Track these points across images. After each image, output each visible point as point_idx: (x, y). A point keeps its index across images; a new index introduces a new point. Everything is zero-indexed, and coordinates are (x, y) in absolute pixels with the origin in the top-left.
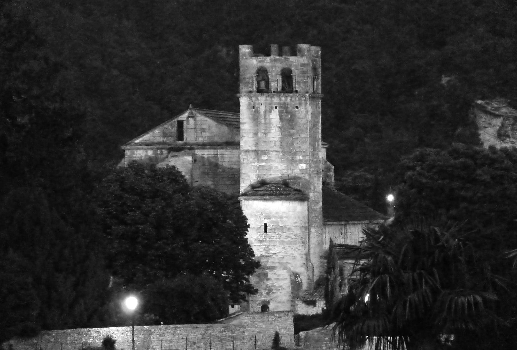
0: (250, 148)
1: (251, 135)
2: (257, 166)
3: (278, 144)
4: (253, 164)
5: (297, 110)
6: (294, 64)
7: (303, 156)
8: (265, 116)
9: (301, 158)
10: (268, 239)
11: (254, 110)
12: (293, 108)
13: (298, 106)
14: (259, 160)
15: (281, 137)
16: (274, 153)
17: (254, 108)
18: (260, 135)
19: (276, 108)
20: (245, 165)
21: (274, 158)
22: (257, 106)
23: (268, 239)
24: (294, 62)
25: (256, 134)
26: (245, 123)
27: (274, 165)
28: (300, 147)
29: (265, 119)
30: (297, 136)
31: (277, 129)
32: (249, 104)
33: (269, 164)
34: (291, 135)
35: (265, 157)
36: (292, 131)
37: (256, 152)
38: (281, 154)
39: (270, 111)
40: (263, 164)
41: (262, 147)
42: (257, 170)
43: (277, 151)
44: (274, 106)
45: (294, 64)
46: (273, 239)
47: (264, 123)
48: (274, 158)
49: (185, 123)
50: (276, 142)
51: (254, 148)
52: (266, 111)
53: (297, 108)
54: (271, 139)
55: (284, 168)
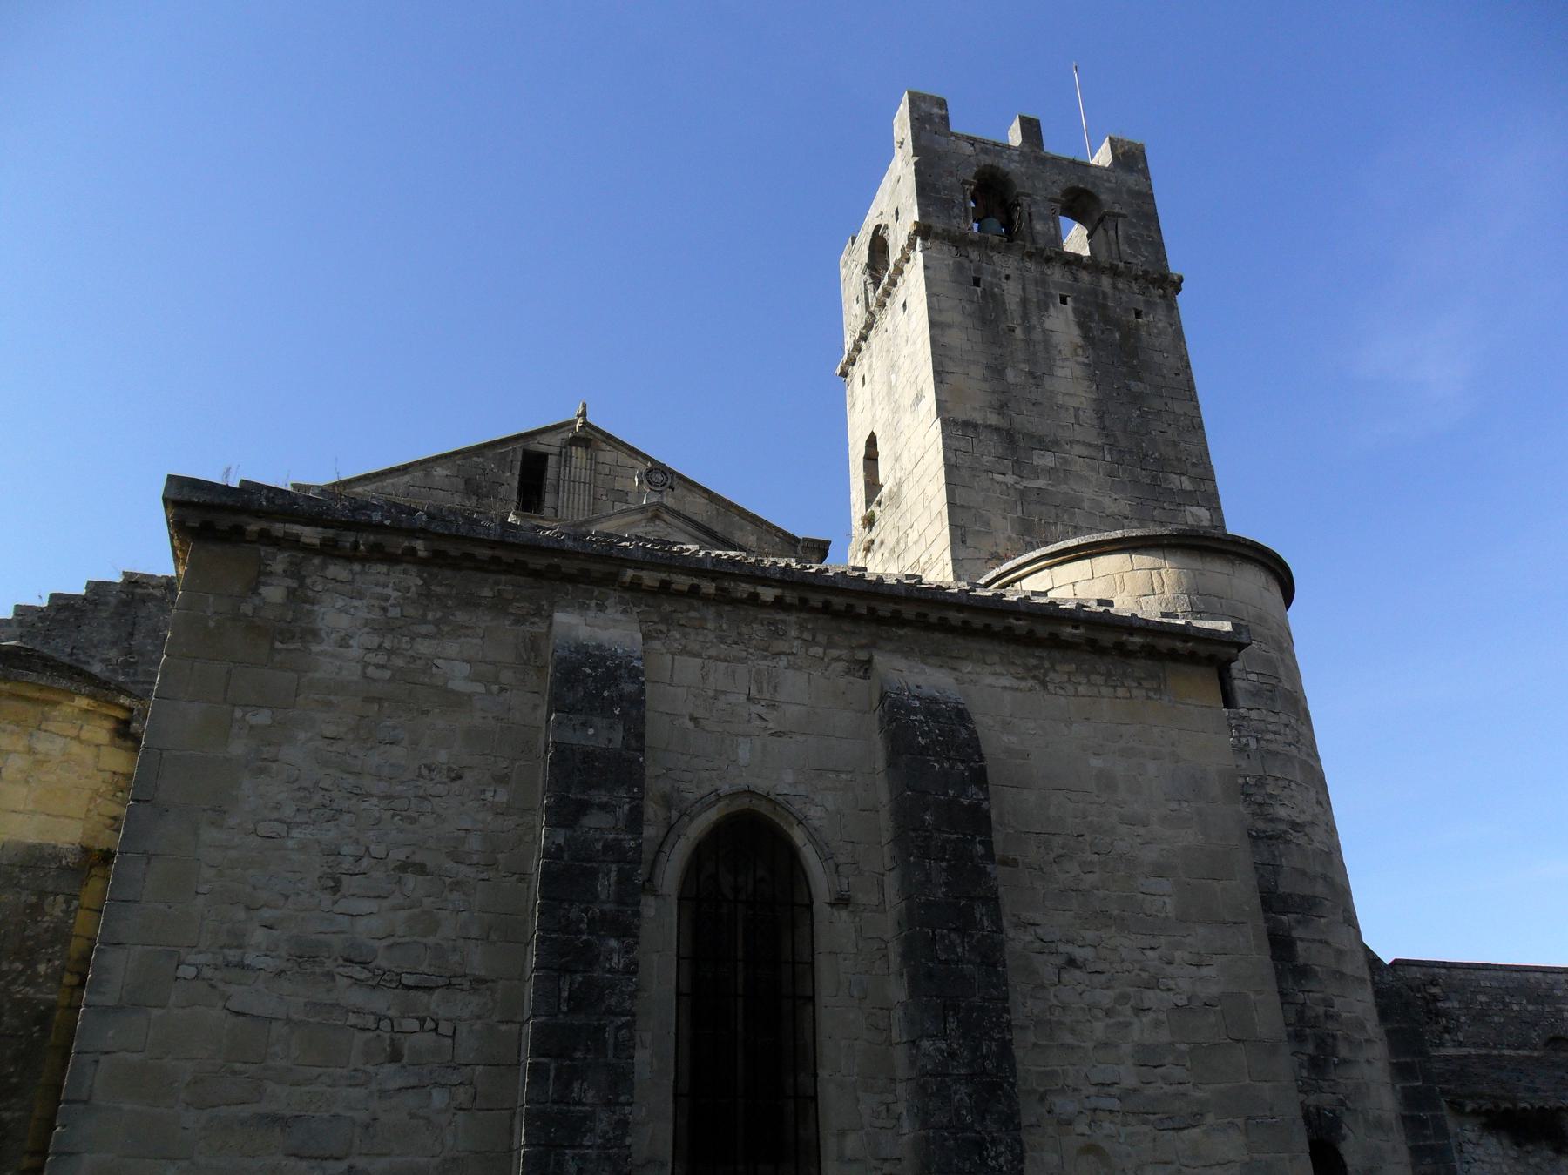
0: (978, 418)
1: (977, 372)
2: (1017, 486)
3: (1088, 416)
4: (997, 477)
5: (1140, 320)
6: (1107, 184)
7: (1192, 479)
8: (1025, 317)
9: (1187, 484)
10: (1253, 744)
11: (979, 289)
12: (1127, 310)
13: (1141, 307)
14: (1019, 466)
15: (1095, 400)
16: (1078, 449)
17: (977, 282)
18: (1011, 375)
19: (1064, 301)
21: (1079, 466)
22: (987, 278)
23: (1253, 744)
24: (1105, 178)
25: (996, 371)
26: (950, 326)
27: (1088, 493)
28: (1175, 444)
29: (1028, 330)
30: (1157, 404)
31: (1079, 371)
32: (960, 268)
33: (1064, 488)
34: (1136, 399)
35: (1047, 460)
36: (1136, 386)
37: (1009, 437)
38: (1108, 458)
39: (1044, 307)
40: (1040, 483)
41: (1027, 421)
42: (1019, 503)
43: (1090, 445)
44: (1057, 293)
45: (1107, 184)
46: (1272, 747)
47: (1022, 340)
49: (552, 461)
50: (1081, 413)
51: (993, 419)
52: (1024, 302)
53: (1138, 314)
54: (1060, 400)
55: (1127, 511)
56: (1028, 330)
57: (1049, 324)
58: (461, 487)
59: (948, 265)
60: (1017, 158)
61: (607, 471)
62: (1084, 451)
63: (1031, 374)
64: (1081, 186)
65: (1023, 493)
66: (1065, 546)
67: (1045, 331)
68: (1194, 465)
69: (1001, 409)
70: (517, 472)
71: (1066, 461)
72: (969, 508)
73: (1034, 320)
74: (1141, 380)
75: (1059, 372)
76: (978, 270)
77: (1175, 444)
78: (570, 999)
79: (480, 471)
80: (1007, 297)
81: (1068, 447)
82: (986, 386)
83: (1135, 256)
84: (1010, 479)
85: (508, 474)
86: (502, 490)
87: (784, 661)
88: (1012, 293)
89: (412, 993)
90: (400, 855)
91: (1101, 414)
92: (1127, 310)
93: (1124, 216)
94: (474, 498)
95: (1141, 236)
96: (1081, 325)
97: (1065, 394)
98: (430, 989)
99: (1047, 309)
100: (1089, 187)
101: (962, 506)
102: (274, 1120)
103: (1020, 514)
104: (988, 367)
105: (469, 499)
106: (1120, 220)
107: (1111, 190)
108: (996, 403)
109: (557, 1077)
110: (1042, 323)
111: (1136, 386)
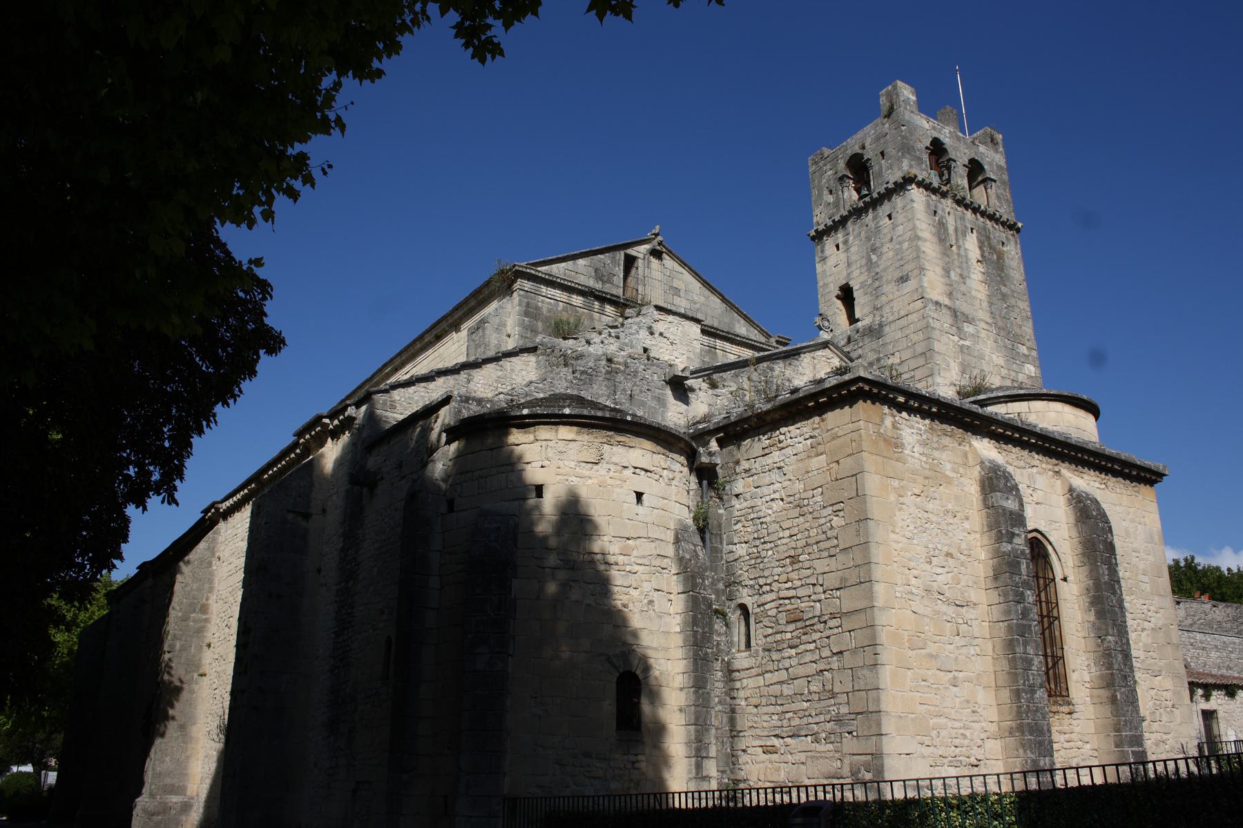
1: (939, 270)
15: (988, 295)
16: (983, 325)
17: (935, 212)
20: (937, 332)
21: (983, 334)
22: (939, 212)
25: (947, 272)
29: (959, 247)
34: (1004, 297)
36: (1004, 289)
37: (954, 313)
38: (994, 332)
39: (964, 235)
41: (962, 306)
43: (987, 323)
45: (987, 159)
48: (983, 334)
51: (947, 301)
52: (956, 230)
55: (1003, 365)
56: (959, 247)
57: (967, 247)
58: (593, 274)
59: (923, 201)
60: (948, 135)
61: (668, 274)
62: (986, 327)
63: (961, 275)
64: (976, 158)
65: (962, 347)
66: (1017, 393)
67: (966, 249)
68: (1028, 340)
69: (950, 295)
70: (622, 268)
71: (978, 331)
72: (940, 354)
73: (961, 243)
74: (1005, 286)
75: (973, 276)
76: (936, 206)
77: (1020, 327)
78: (1022, 614)
79: (603, 265)
80: (949, 225)
81: (978, 322)
82: (942, 280)
83: (1000, 208)
84: (956, 338)
85: (617, 269)
86: (615, 278)
87: (1035, 470)
88: (951, 222)
89: (959, 608)
90: (945, 549)
91: (991, 304)
92: (998, 242)
93: (995, 181)
94: (600, 283)
95: (1003, 195)
96: (980, 248)
97: (976, 290)
98: (963, 606)
99: (966, 236)
100: (979, 159)
101: (938, 352)
102: (931, 656)
103: (960, 360)
104: (943, 269)
105: (597, 282)
106: (993, 183)
107: (989, 163)
108: (948, 292)
109: (1023, 644)
110: (964, 244)
111: (1004, 289)
